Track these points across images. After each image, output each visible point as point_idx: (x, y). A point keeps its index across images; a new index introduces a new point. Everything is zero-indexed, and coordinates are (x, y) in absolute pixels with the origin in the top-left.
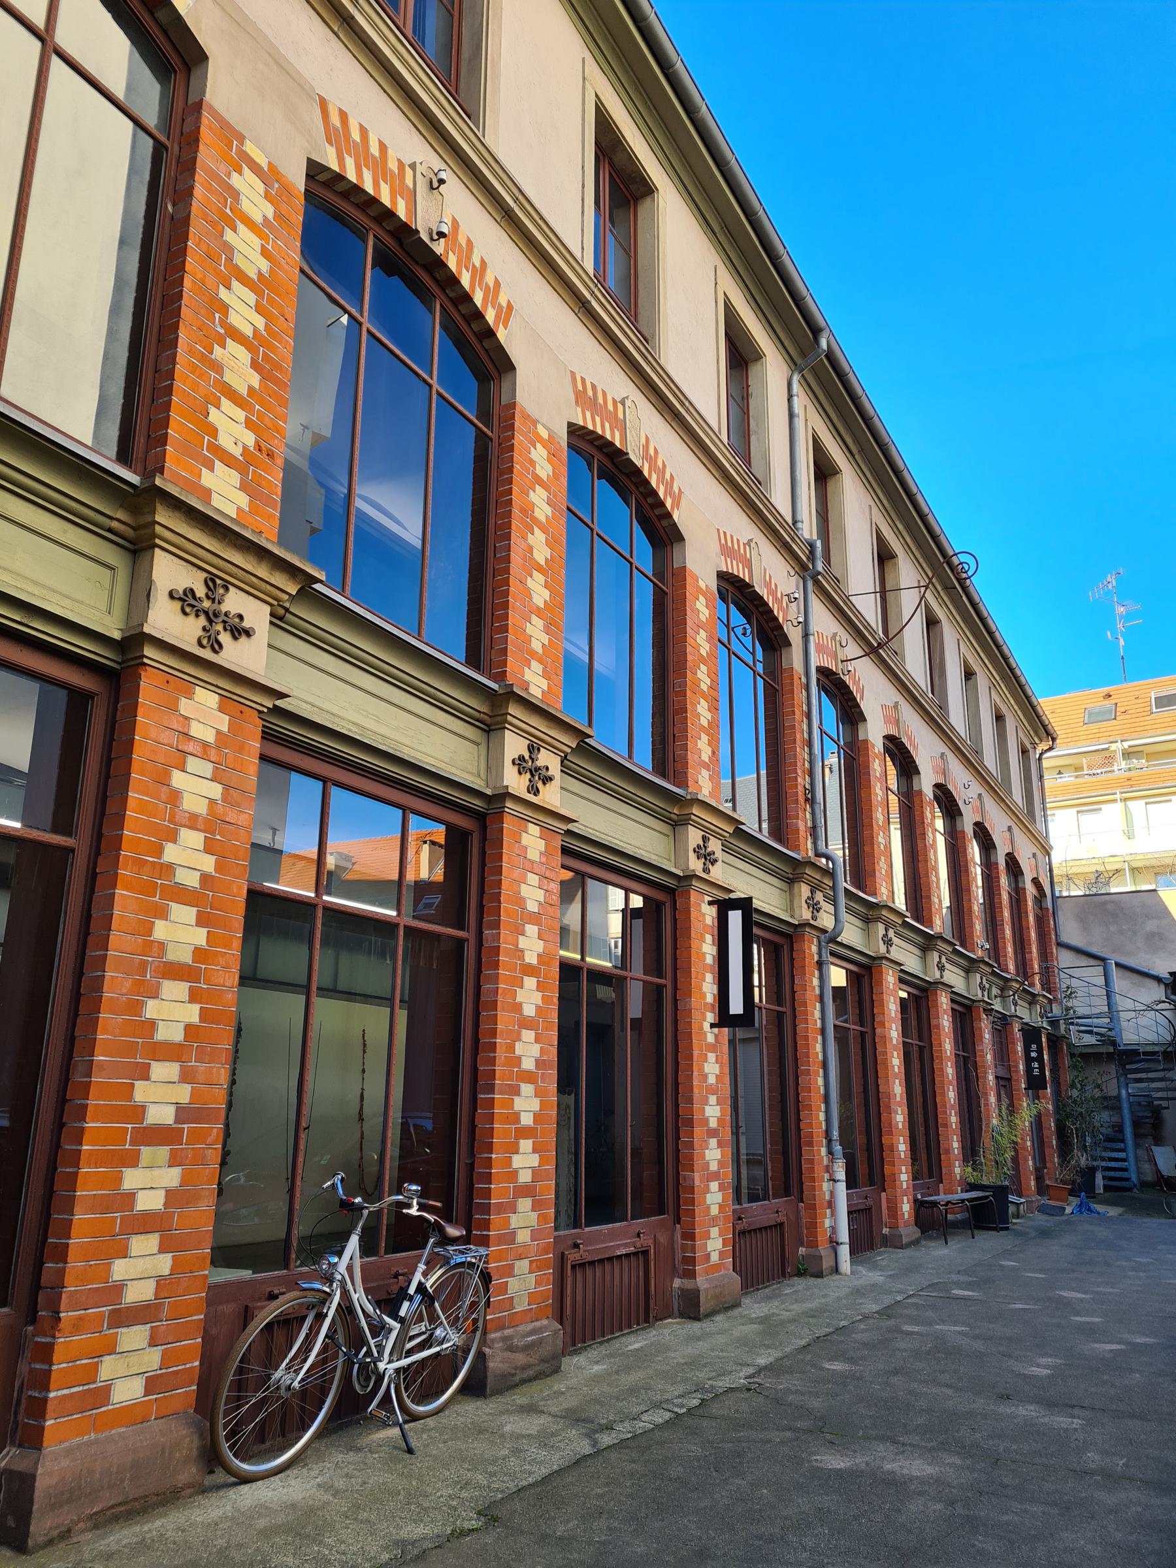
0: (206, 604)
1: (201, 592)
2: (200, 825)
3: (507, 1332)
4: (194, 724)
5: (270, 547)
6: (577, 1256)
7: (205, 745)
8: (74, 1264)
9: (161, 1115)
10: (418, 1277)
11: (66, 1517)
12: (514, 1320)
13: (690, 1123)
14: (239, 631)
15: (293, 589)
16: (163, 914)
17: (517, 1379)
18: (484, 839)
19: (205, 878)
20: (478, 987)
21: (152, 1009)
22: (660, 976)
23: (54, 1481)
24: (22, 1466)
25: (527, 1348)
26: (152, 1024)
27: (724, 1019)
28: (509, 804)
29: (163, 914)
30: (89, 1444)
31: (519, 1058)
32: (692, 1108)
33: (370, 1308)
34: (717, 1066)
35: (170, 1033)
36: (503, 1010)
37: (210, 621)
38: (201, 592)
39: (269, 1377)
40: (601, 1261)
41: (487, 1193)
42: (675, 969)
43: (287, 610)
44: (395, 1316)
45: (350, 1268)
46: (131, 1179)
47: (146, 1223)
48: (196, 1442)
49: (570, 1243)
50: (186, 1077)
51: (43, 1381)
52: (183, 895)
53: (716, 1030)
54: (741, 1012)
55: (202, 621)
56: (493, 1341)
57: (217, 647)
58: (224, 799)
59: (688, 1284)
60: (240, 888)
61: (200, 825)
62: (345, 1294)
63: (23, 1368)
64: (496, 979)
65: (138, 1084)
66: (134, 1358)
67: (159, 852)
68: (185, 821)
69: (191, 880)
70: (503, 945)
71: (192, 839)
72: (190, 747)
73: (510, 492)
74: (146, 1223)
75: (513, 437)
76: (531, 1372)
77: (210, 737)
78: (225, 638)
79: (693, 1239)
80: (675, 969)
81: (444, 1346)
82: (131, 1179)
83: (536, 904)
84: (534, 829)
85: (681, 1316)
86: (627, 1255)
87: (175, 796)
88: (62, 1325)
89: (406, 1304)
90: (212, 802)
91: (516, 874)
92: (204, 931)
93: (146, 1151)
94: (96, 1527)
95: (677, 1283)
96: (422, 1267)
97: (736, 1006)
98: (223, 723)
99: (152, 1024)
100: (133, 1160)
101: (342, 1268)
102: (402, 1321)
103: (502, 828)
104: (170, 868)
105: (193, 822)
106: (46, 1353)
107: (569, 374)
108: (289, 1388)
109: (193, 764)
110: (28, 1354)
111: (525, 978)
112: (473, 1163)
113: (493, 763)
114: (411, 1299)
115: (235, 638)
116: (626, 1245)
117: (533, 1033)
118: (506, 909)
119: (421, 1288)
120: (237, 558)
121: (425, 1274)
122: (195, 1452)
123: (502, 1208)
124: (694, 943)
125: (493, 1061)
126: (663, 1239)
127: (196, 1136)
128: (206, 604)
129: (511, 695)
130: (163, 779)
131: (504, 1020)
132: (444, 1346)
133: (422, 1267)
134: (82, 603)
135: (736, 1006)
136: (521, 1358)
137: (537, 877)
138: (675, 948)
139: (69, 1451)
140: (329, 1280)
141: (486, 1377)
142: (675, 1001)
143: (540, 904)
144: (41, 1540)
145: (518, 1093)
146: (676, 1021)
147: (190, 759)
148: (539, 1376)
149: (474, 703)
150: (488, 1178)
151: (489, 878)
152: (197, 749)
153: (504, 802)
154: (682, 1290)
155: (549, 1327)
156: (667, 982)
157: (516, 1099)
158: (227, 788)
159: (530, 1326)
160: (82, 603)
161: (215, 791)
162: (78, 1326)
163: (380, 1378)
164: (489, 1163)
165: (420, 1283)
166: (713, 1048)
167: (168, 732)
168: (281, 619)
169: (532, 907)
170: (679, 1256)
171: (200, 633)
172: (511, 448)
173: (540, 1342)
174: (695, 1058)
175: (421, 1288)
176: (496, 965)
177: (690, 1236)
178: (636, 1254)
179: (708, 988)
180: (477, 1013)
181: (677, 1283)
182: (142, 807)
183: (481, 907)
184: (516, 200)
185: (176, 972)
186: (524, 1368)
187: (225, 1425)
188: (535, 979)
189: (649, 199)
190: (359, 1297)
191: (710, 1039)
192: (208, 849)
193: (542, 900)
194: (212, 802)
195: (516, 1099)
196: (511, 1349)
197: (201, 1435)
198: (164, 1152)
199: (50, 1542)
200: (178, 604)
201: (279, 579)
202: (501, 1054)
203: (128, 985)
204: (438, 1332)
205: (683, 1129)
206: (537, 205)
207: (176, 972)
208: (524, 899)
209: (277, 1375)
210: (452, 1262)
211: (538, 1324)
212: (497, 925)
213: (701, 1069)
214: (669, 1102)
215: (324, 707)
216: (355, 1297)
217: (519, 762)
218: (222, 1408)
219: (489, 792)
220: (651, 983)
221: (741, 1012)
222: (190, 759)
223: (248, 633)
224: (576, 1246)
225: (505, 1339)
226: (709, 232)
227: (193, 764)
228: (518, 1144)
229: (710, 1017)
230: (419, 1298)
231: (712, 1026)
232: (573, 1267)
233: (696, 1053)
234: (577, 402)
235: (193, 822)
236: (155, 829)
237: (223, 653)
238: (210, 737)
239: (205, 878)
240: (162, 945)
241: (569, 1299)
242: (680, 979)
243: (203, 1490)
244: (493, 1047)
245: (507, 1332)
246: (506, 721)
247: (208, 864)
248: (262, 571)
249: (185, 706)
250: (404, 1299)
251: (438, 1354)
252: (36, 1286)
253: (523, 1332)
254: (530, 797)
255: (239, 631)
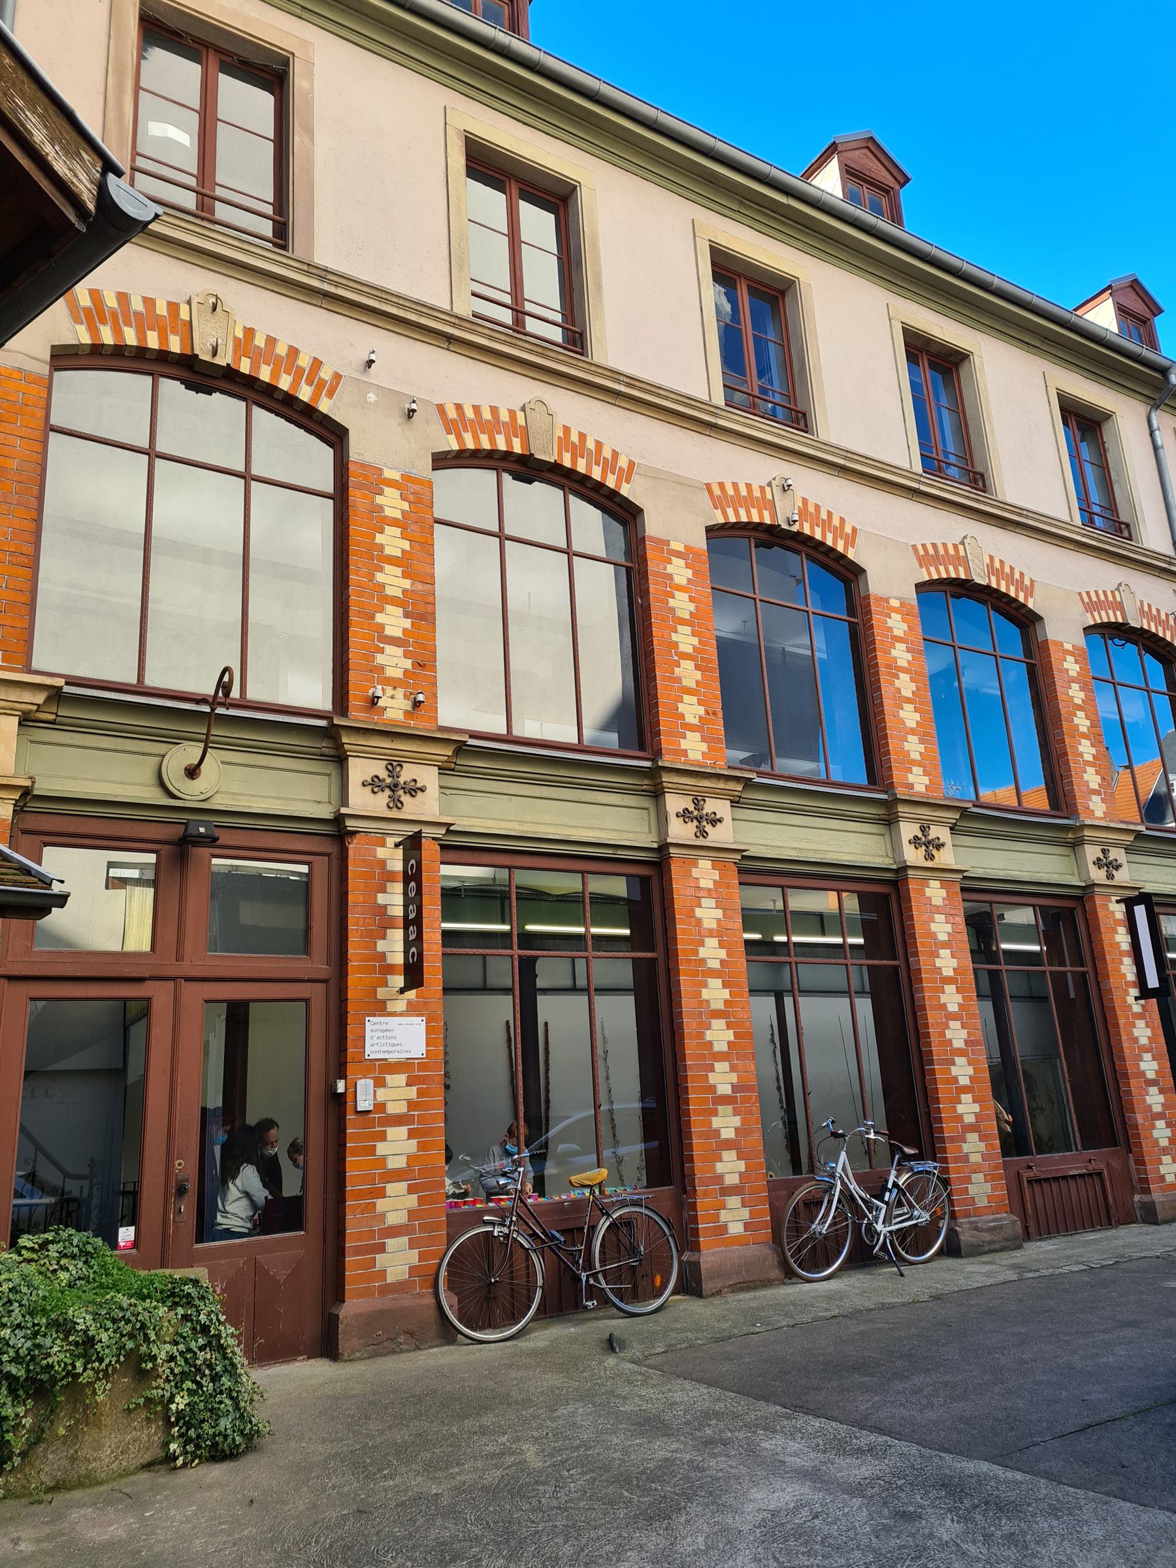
0: (696, 813)
1: (691, 808)
2: (715, 934)
3: (973, 1219)
4: (701, 880)
5: (722, 772)
6: (1032, 1174)
7: (709, 890)
8: (698, 1164)
9: (724, 1089)
10: (892, 1179)
11: (718, 1284)
12: (978, 1212)
13: (1126, 1076)
14: (715, 821)
15: (740, 788)
16: (705, 985)
17: (986, 1249)
18: (899, 898)
19: (722, 962)
20: (912, 997)
21: (709, 1036)
22: (1082, 966)
23: (709, 1266)
24: (693, 1259)
25: (990, 1230)
26: (710, 1043)
27: (1145, 993)
28: (910, 872)
29: (705, 985)
30: (722, 1251)
31: (950, 1041)
32: (1125, 1065)
33: (863, 1194)
34: (1149, 1030)
35: (721, 1046)
36: (931, 1010)
37: (699, 822)
38: (691, 808)
39: (810, 1227)
40: (1056, 1179)
41: (941, 1130)
42: (1093, 958)
43: (740, 797)
44: (882, 1201)
45: (844, 1169)
46: (716, 1122)
47: (728, 1145)
48: (776, 1259)
49: (1025, 1165)
50: (733, 1069)
51: (695, 1220)
52: (713, 973)
53: (1142, 1002)
54: (1157, 986)
55: (695, 823)
56: (962, 1223)
57: (704, 834)
58: (724, 916)
59: (1146, 1198)
60: (742, 964)
61: (715, 934)
62: (843, 1183)
63: (685, 1215)
64: (922, 990)
65: (710, 1074)
66: (735, 1212)
67: (696, 953)
68: (707, 934)
69: (714, 964)
70: (923, 967)
71: (711, 942)
72: (701, 894)
73: (875, 657)
74: (728, 1145)
75: (871, 619)
76: (997, 1246)
77: (711, 885)
78: (708, 828)
79: (1144, 1164)
80: (1093, 958)
81: (920, 1221)
82: (716, 1122)
83: (946, 935)
84: (935, 884)
85: (1144, 1222)
86: (1081, 1176)
87: (699, 922)
88: (698, 1193)
89: (887, 1194)
90: (718, 920)
91: (926, 917)
92: (727, 991)
93: (720, 1108)
94: (733, 1291)
95: (1137, 1198)
96: (893, 1173)
97: (1153, 982)
98: (716, 875)
99: (710, 1043)
100: (715, 1113)
101: (839, 1169)
102: (887, 1203)
103: (908, 890)
104: (703, 961)
105: (710, 933)
106: (694, 1206)
107: (910, 549)
108: (820, 1233)
109: (704, 902)
110: (686, 1207)
111: (946, 986)
112: (929, 1112)
113: (896, 846)
114: (890, 1191)
115: (714, 826)
116: (1077, 1168)
117: (959, 1023)
118: (922, 943)
119: (895, 1185)
120: (706, 783)
121: (897, 1177)
122: (776, 1263)
123: (953, 1139)
124: (1106, 937)
125: (929, 1044)
126: (1116, 1164)
127: (745, 1100)
128: (696, 813)
129: (897, 801)
130: (691, 914)
131: (932, 1017)
132: (920, 1221)
133: (893, 1173)
134: (637, 832)
135: (1153, 982)
136: (987, 1236)
137: (943, 916)
138: (1091, 942)
139: (713, 1254)
140: (833, 1176)
141: (960, 1245)
142: (1098, 983)
143: (949, 934)
144: (709, 1293)
145: (954, 1064)
146: (1101, 999)
147: (703, 900)
148: (1003, 1249)
149: (873, 811)
150: (940, 1120)
151: (907, 923)
152: (706, 894)
153: (906, 871)
154: (1141, 1203)
155: (1007, 1218)
156: (1088, 969)
157: (953, 1068)
158: (725, 910)
159: (992, 1217)
160: (637, 832)
161: (719, 913)
162: (706, 1194)
163: (879, 1235)
164: (939, 1110)
165: (894, 1182)
166: (1140, 1016)
167: (689, 889)
168: (738, 803)
169: (943, 937)
170: (1135, 1178)
171: (695, 830)
172: (872, 627)
173: (1001, 1227)
174: (1121, 1026)
175: (895, 1185)
176: (920, 981)
177: (1141, 1162)
178: (1090, 1175)
179: (1128, 969)
180: (915, 1014)
181: (1137, 1198)
182: (684, 932)
183: (905, 943)
184: (846, 458)
185: (717, 1014)
186: (990, 1243)
187: (790, 1250)
188: (954, 986)
189: (966, 362)
190: (853, 1186)
191: (1137, 1008)
192: (721, 946)
193: (950, 931)
194: (718, 920)
195: (953, 1068)
196: (976, 1229)
197: (778, 1254)
198: (729, 1108)
199: (713, 1295)
200: (682, 819)
201: (731, 786)
202: (934, 1039)
203: (695, 1024)
204: (916, 1213)
205: (1121, 1082)
206: (861, 452)
207: (717, 1014)
208: (935, 933)
209: (814, 1226)
210: (916, 1170)
211: (999, 1216)
212: (916, 954)
213: (1130, 1034)
214: (1106, 1061)
215: (774, 844)
216: (852, 1187)
217: (915, 841)
218: (785, 1241)
219: (894, 867)
220: (1078, 972)
221: (1157, 986)
222: (703, 900)
223: (720, 821)
224: (1030, 1167)
225: (971, 1223)
226: (1031, 349)
227: (704, 902)
228: (959, 1097)
229: (1134, 992)
230: (895, 1191)
231: (1136, 999)
232: (1029, 1182)
233: (1122, 1022)
234: (921, 566)
235: (710, 933)
236: (692, 942)
237: (709, 838)
238: (711, 885)
239: (722, 962)
240: (707, 1001)
241: (1029, 1203)
242: (1099, 966)
243: (785, 1284)
244: (928, 1035)
245: (973, 1219)
246: (899, 817)
247: (722, 954)
248: (721, 785)
249: (695, 872)
250: (886, 1191)
251: (915, 1225)
252: (684, 1176)
253: (987, 1220)
254: (929, 864)
255: (715, 821)
